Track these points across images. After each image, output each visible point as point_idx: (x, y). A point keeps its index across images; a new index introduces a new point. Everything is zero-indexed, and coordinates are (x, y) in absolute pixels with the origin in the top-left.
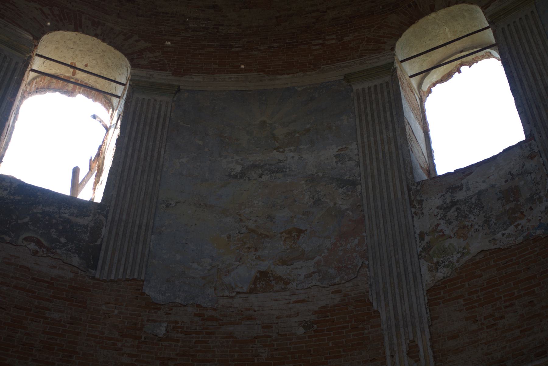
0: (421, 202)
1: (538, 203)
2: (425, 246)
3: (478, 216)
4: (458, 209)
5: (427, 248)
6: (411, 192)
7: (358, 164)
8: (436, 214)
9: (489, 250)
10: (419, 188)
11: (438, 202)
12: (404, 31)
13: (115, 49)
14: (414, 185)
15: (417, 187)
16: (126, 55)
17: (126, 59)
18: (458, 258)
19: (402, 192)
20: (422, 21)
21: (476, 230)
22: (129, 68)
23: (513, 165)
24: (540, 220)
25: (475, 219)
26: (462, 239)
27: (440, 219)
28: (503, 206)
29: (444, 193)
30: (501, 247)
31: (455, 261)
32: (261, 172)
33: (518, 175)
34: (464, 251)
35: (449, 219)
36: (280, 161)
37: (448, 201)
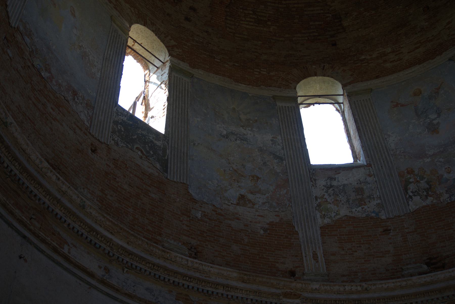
0: (315, 180)
1: (373, 200)
2: (318, 204)
3: (344, 197)
4: (333, 190)
5: (319, 205)
6: (310, 173)
7: (283, 149)
8: (323, 189)
9: (349, 216)
10: (314, 172)
11: (324, 183)
12: (301, 80)
13: (161, 41)
14: (311, 169)
15: (313, 171)
16: (166, 47)
17: (166, 49)
18: (334, 215)
19: (306, 172)
20: (309, 79)
21: (343, 204)
22: (167, 54)
23: (361, 176)
24: (374, 209)
25: (342, 198)
26: (336, 206)
27: (325, 192)
28: (356, 196)
29: (326, 179)
30: (355, 216)
31: (333, 217)
32: (236, 138)
33: (363, 182)
34: (337, 213)
35: (329, 194)
36: (244, 134)
37: (329, 184)
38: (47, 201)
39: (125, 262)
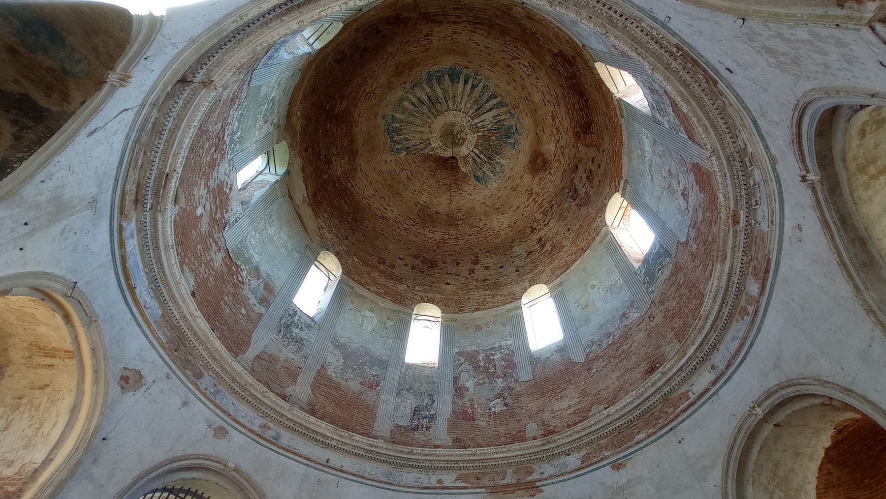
38: (658, 396)
39: (708, 350)
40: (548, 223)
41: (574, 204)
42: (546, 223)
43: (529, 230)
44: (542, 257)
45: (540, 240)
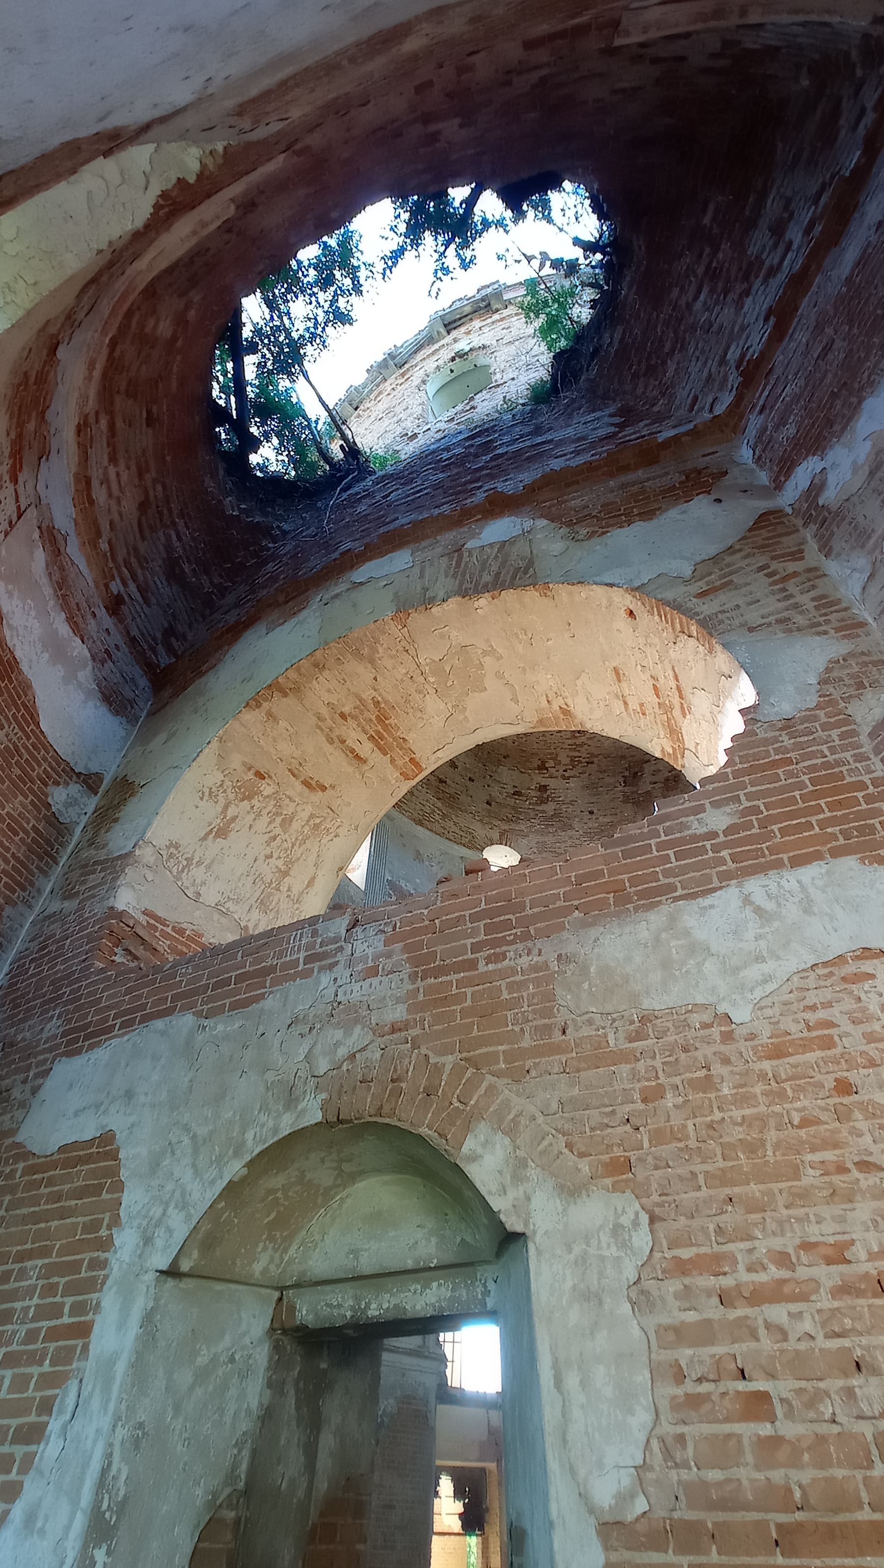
40: (568, 778)
41: (620, 788)
42: (567, 774)
43: (536, 763)
44: (532, 814)
45: (543, 788)
